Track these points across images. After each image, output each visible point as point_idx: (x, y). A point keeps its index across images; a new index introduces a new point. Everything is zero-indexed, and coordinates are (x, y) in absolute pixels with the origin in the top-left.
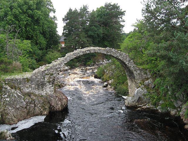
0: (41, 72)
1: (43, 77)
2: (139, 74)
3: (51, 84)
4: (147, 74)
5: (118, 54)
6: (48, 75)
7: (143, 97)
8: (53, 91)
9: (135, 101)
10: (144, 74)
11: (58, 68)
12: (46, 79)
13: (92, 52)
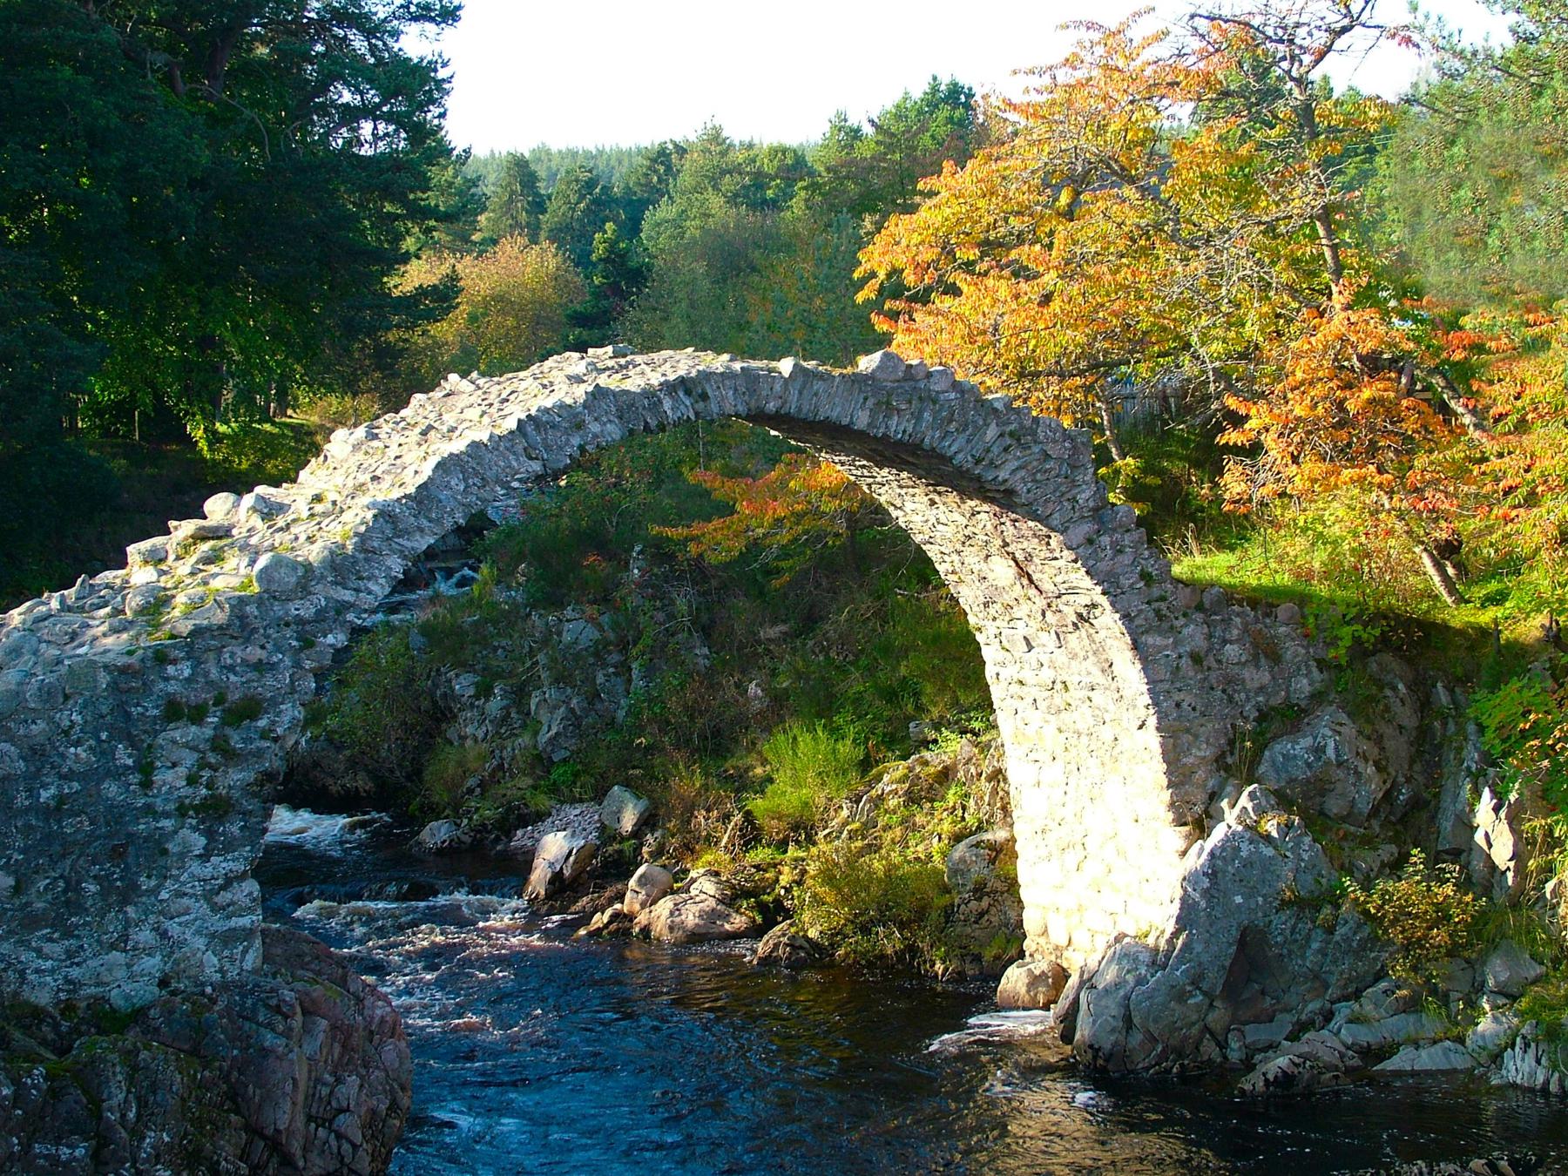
0: (104, 679)
1: (124, 756)
2: (1196, 659)
3: (229, 847)
4: (1275, 657)
5: (992, 432)
6: (197, 715)
7: (1282, 922)
8: (248, 934)
9: (1196, 982)
10: (1255, 661)
11: (320, 615)
12: (170, 779)
13: (728, 401)
